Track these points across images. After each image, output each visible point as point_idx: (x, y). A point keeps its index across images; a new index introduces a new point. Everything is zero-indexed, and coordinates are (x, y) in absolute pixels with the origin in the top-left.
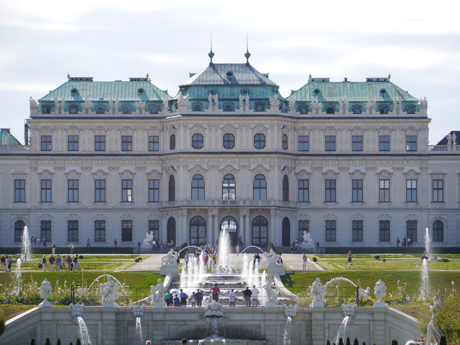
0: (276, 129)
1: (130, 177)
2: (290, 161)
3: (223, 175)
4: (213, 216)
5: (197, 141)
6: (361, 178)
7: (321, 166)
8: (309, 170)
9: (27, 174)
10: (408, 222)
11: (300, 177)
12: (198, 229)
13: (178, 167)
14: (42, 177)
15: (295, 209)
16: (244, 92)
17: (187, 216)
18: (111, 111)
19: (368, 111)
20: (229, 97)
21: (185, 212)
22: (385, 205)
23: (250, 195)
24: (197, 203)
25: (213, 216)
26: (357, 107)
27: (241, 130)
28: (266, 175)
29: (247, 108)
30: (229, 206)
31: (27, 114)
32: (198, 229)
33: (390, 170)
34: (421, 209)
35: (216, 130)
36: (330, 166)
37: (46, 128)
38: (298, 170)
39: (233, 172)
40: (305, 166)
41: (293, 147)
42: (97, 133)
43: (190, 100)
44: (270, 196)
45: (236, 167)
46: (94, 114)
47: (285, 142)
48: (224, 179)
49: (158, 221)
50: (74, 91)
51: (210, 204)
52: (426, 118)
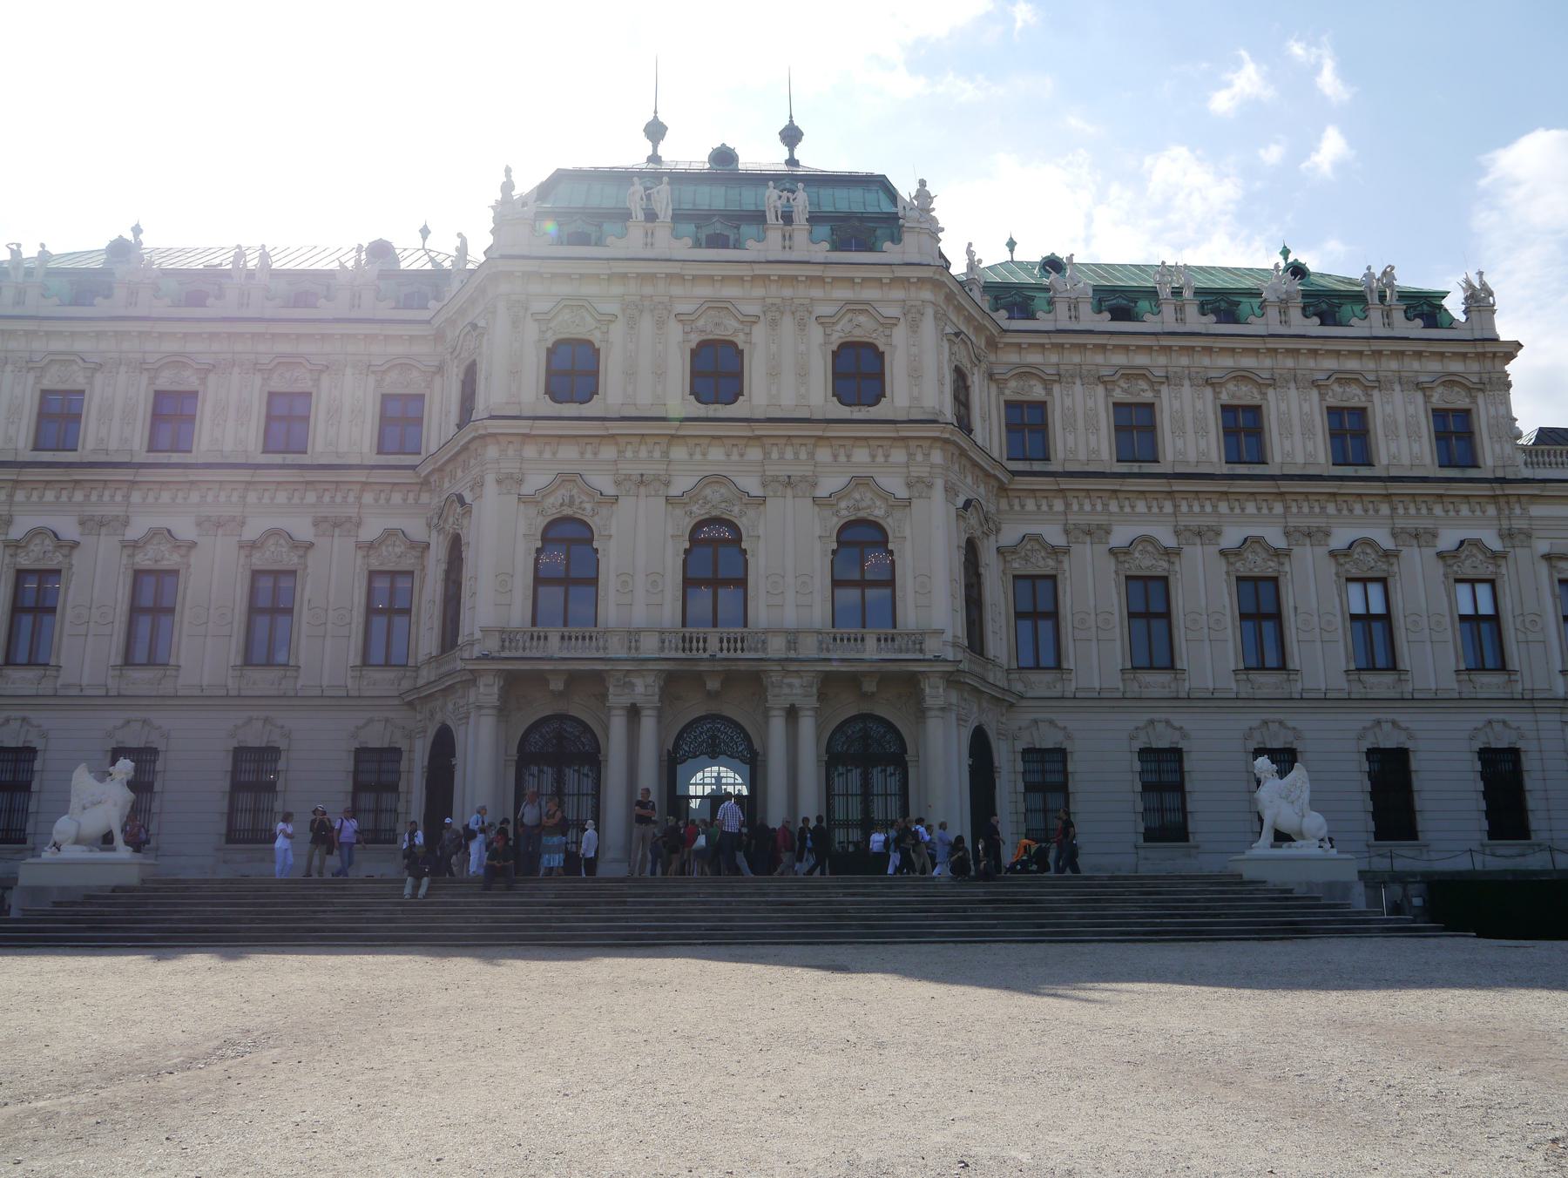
0: (928, 326)
1: (290, 560)
2: (982, 490)
3: (688, 523)
4: (634, 712)
6: (1270, 573)
7: (1102, 519)
11: (1018, 566)
12: (559, 781)
13: (479, 484)
17: (503, 712)
19: (1272, 313)
21: (488, 692)
24: (554, 646)
25: (634, 712)
27: (774, 323)
28: (889, 524)
30: (713, 658)
32: (559, 781)
34: (1531, 702)
36: (1139, 523)
38: (1010, 534)
39: (736, 509)
44: (910, 616)
45: (752, 485)
49: (398, 751)
51: (616, 648)
52: (1496, 340)
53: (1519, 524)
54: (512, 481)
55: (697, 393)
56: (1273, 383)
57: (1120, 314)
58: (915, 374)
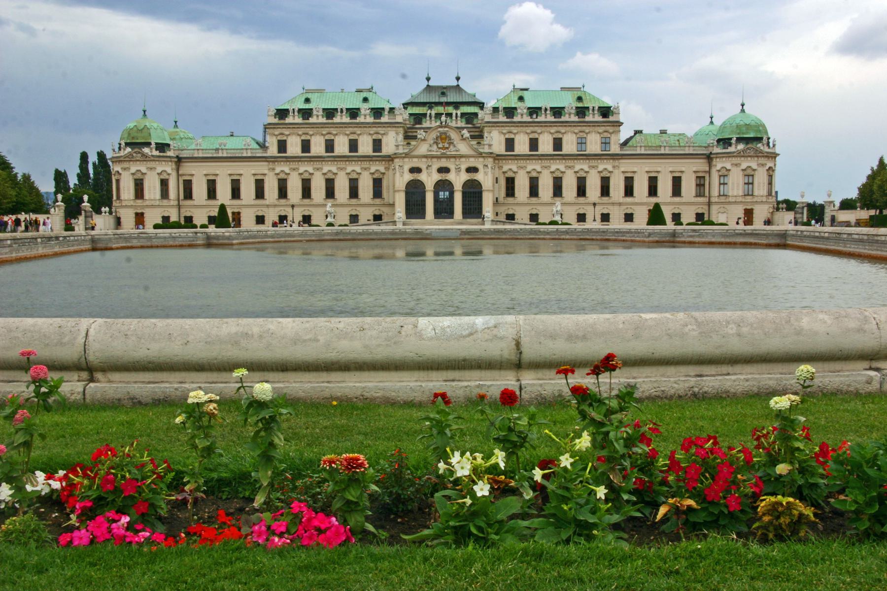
8: (515, 169)
9: (265, 175)
26: (557, 112)
33: (587, 169)
34: (613, 204)
36: (534, 166)
40: (510, 166)
50: (307, 100)
52: (618, 122)
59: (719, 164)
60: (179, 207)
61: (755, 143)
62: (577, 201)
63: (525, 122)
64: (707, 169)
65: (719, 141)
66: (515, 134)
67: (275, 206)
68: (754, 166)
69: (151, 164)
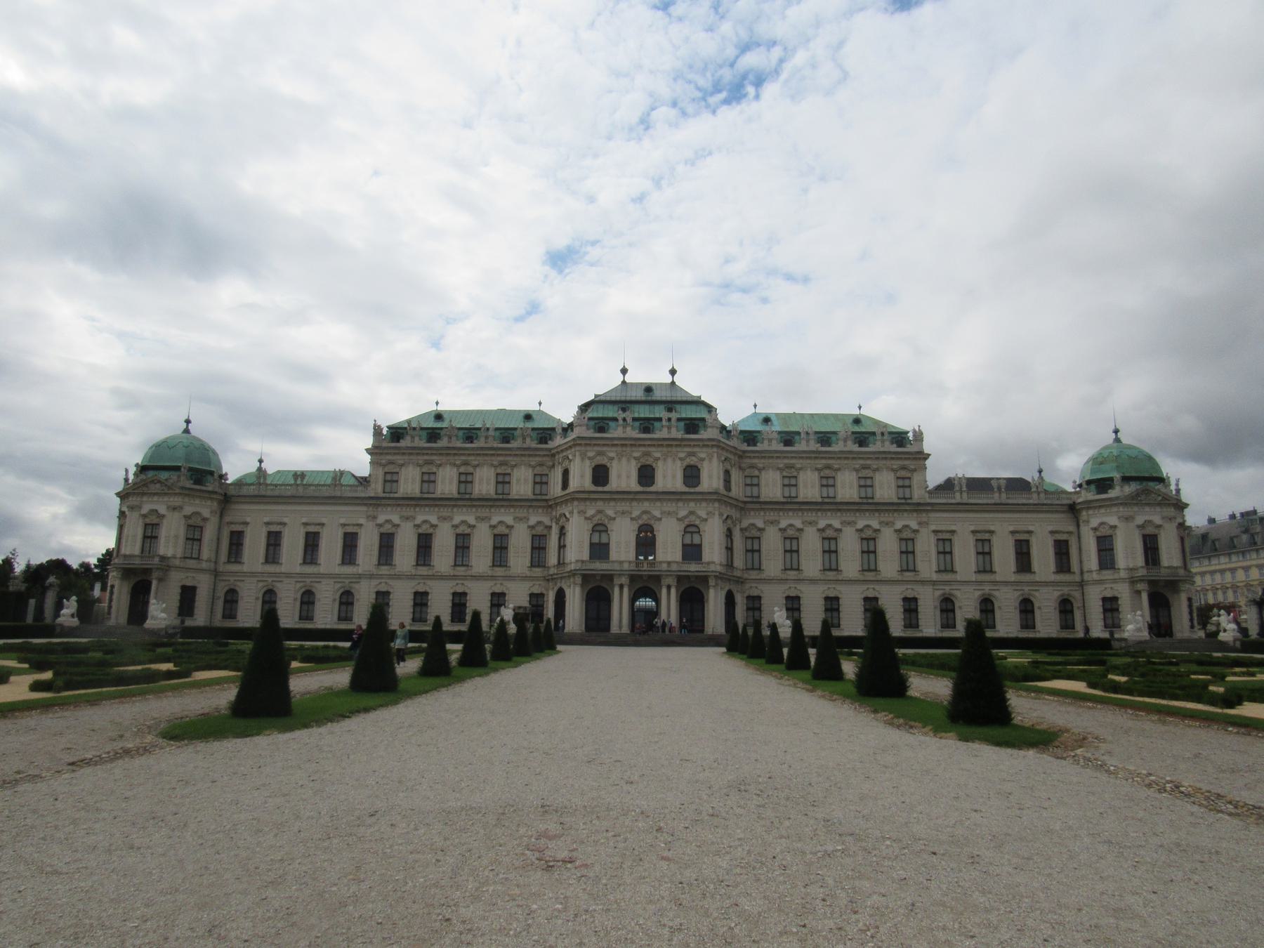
0: (715, 460)
3: (636, 527)
4: (621, 587)
5: (600, 475)
8: (760, 524)
10: (906, 599)
11: (747, 534)
13: (571, 513)
14: (383, 530)
15: (740, 581)
16: (670, 410)
17: (582, 586)
18: (482, 439)
19: (841, 443)
20: (648, 416)
21: (579, 580)
22: (870, 576)
23: (677, 555)
25: (621, 587)
26: (825, 438)
29: (673, 430)
31: (369, 442)
33: (877, 527)
34: (923, 582)
35: (628, 460)
37: (391, 463)
38: (745, 523)
41: (737, 491)
42: (462, 469)
43: (590, 419)
45: (657, 513)
46: (459, 444)
47: (727, 482)
48: (640, 531)
51: (617, 567)
52: (921, 452)
53: (925, 520)
54: (581, 512)
55: (640, 483)
56: (839, 469)
57: (788, 442)
58: (710, 477)
59: (1094, 519)
60: (216, 573)
61: (1151, 484)
62: (861, 578)
63: (776, 452)
64: (1072, 528)
65: (1089, 482)
66: (760, 470)
67: (371, 576)
68: (1157, 520)
69: (177, 501)
